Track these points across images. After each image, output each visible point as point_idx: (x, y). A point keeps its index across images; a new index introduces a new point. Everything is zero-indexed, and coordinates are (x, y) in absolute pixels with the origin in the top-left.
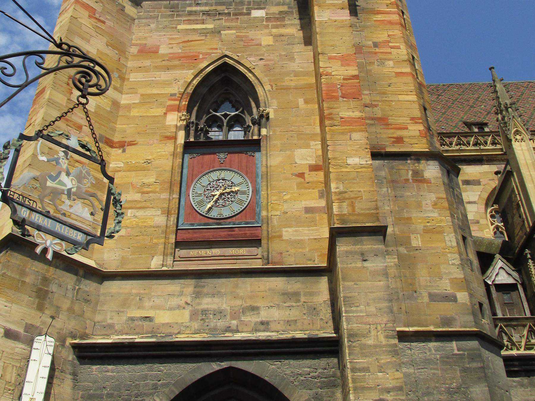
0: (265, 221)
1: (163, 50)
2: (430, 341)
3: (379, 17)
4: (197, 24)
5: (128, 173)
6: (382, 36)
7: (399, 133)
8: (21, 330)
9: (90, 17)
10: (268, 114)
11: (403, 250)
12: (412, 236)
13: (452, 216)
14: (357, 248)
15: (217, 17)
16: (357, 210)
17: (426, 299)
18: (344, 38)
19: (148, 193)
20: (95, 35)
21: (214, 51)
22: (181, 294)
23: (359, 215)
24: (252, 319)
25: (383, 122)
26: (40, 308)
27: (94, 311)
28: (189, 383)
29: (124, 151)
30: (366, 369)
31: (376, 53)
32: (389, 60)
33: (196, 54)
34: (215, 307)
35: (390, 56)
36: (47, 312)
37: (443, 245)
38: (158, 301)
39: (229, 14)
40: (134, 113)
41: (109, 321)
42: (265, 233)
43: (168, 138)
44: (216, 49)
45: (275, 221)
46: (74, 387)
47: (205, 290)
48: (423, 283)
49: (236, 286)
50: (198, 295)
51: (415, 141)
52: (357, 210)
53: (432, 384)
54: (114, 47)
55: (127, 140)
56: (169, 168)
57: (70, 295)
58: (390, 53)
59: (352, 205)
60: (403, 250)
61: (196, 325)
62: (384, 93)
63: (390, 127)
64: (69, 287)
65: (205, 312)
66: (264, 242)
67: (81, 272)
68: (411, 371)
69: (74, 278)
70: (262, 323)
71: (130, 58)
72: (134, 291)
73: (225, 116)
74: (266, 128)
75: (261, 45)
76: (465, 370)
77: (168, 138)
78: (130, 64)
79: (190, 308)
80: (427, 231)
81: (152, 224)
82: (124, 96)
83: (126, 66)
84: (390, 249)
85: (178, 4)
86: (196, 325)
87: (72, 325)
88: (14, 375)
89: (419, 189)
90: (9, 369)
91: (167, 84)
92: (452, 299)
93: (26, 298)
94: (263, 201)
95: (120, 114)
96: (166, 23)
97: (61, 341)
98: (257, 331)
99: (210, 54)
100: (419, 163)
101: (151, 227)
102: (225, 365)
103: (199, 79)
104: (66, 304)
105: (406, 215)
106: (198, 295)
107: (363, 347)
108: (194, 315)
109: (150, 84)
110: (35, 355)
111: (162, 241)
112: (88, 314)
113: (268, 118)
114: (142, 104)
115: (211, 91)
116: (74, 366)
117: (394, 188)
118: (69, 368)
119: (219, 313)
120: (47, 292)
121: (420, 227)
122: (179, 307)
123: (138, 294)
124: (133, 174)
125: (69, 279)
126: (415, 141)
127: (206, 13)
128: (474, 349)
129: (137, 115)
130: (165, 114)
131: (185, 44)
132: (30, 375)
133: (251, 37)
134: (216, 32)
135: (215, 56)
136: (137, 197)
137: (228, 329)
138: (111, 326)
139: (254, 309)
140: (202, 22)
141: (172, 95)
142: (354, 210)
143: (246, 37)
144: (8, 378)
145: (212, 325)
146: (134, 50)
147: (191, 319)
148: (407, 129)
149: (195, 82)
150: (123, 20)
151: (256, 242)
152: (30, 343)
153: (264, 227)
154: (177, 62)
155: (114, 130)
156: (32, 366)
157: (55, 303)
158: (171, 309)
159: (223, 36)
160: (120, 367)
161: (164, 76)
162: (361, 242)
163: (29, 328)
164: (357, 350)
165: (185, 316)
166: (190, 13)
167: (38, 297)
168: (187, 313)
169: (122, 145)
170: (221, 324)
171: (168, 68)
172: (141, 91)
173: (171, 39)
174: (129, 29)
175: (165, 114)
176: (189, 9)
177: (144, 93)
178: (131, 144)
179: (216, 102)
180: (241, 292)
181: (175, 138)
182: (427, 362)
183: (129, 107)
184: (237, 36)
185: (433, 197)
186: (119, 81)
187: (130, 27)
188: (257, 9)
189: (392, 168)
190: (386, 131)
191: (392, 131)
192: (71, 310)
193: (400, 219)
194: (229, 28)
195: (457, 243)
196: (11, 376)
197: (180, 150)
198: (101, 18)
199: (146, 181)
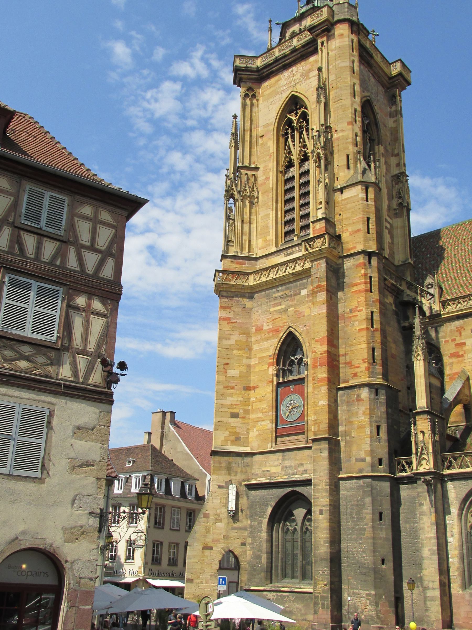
0: (306, 422)
1: (265, 328)
2: (353, 480)
3: (355, 289)
4: (278, 306)
5: (256, 403)
6: (354, 304)
7: (356, 370)
8: (224, 484)
9: (228, 323)
10: (307, 362)
11: (348, 438)
12: (352, 431)
13: (371, 417)
14: (318, 447)
15: (286, 300)
16: (321, 429)
17: (354, 461)
18: (323, 326)
19: (264, 413)
20: (232, 333)
21: (286, 324)
22: (278, 460)
23: (321, 431)
24: (301, 469)
25: (349, 365)
26: (229, 474)
27: (251, 468)
28: (281, 496)
29: (255, 392)
30: (318, 498)
31: (350, 317)
32: (356, 321)
33: (277, 328)
34: (289, 464)
35: (358, 318)
36: (232, 475)
37: (364, 434)
38: (271, 463)
39: (291, 295)
40: (257, 369)
41: (257, 473)
42: (306, 429)
43: (270, 382)
44: (286, 323)
45: (309, 423)
46: (248, 499)
47: (286, 457)
48: (354, 454)
49: (296, 455)
50: (283, 460)
51: (363, 374)
52: (321, 429)
53: (351, 498)
54: (243, 334)
55: (255, 385)
56: (271, 399)
57: (240, 466)
58: (357, 315)
59: (319, 426)
60: (348, 438)
61: (283, 473)
62: (352, 345)
63: (353, 367)
64: (239, 463)
65: (286, 467)
66: (306, 433)
67: (243, 455)
68: (345, 492)
69: (241, 458)
70: (305, 471)
71: (253, 335)
72: (263, 459)
73: (296, 359)
74: (307, 370)
75: (304, 316)
76: (364, 492)
77: (270, 382)
78: (253, 339)
79: (281, 465)
80: (359, 427)
81: (266, 428)
82: (252, 360)
83: (251, 341)
84: (343, 438)
85: (269, 293)
86: (283, 473)
87: (243, 477)
88: (224, 500)
89: (358, 405)
90: (222, 499)
91: (267, 349)
92: (364, 460)
93: (223, 472)
94: (306, 412)
95: (252, 371)
96: (265, 308)
97: (240, 484)
98: (303, 474)
99: (283, 327)
100: (360, 390)
101: (266, 430)
102: (291, 489)
103: (280, 344)
104: (239, 470)
105: (351, 420)
106: (283, 460)
107: (318, 489)
108: (282, 468)
109: (261, 350)
110: (230, 492)
111: (271, 436)
112: (249, 470)
113: (307, 364)
114: (259, 363)
115: (288, 346)
116: (246, 491)
117: (348, 406)
118: (245, 493)
119: (290, 467)
120: (231, 467)
121: (356, 426)
122: (278, 465)
123: (264, 461)
124: (258, 403)
125: (239, 460)
126: (363, 374)
127: (281, 297)
128: (369, 483)
129: (258, 370)
130: (268, 368)
131: (273, 322)
132: (230, 499)
133: (301, 311)
134: (286, 310)
135: (286, 327)
136: (260, 415)
137: (294, 474)
138: (257, 475)
139: (302, 464)
140: (279, 304)
141: (270, 356)
142: (319, 429)
143: (299, 311)
144: (222, 501)
145: (288, 472)
146: (253, 330)
147: (282, 470)
148: (359, 367)
149: (279, 346)
150: (245, 314)
151: (303, 433)
152: (228, 488)
153: (306, 426)
154: (271, 335)
155: (250, 381)
156: (230, 496)
157: (235, 471)
158: (275, 466)
159: (289, 313)
160: (260, 491)
161: (266, 344)
162: (320, 445)
163: (226, 483)
164: (315, 491)
165: (279, 469)
166: (275, 298)
167: (228, 470)
168: (280, 467)
169: (254, 388)
170: (291, 472)
171: (267, 339)
172: (259, 355)
173: (268, 319)
174: (250, 318)
175: (268, 368)
176: (274, 296)
177: (260, 356)
178: (257, 387)
179: (292, 351)
180: (298, 458)
181: (273, 382)
182: (351, 489)
183: (255, 366)
184: (295, 312)
185: (363, 408)
186: (248, 352)
187: (250, 316)
188: (303, 289)
189: (348, 395)
190: (350, 370)
191: (353, 369)
192: (242, 471)
193: (349, 422)
194: (291, 306)
195: (370, 432)
196: (224, 501)
197: (274, 388)
198: (234, 321)
199: (263, 407)
